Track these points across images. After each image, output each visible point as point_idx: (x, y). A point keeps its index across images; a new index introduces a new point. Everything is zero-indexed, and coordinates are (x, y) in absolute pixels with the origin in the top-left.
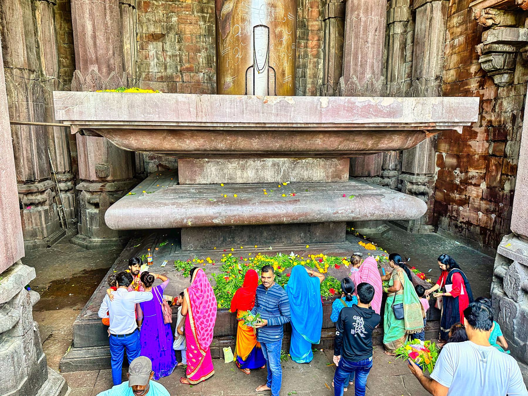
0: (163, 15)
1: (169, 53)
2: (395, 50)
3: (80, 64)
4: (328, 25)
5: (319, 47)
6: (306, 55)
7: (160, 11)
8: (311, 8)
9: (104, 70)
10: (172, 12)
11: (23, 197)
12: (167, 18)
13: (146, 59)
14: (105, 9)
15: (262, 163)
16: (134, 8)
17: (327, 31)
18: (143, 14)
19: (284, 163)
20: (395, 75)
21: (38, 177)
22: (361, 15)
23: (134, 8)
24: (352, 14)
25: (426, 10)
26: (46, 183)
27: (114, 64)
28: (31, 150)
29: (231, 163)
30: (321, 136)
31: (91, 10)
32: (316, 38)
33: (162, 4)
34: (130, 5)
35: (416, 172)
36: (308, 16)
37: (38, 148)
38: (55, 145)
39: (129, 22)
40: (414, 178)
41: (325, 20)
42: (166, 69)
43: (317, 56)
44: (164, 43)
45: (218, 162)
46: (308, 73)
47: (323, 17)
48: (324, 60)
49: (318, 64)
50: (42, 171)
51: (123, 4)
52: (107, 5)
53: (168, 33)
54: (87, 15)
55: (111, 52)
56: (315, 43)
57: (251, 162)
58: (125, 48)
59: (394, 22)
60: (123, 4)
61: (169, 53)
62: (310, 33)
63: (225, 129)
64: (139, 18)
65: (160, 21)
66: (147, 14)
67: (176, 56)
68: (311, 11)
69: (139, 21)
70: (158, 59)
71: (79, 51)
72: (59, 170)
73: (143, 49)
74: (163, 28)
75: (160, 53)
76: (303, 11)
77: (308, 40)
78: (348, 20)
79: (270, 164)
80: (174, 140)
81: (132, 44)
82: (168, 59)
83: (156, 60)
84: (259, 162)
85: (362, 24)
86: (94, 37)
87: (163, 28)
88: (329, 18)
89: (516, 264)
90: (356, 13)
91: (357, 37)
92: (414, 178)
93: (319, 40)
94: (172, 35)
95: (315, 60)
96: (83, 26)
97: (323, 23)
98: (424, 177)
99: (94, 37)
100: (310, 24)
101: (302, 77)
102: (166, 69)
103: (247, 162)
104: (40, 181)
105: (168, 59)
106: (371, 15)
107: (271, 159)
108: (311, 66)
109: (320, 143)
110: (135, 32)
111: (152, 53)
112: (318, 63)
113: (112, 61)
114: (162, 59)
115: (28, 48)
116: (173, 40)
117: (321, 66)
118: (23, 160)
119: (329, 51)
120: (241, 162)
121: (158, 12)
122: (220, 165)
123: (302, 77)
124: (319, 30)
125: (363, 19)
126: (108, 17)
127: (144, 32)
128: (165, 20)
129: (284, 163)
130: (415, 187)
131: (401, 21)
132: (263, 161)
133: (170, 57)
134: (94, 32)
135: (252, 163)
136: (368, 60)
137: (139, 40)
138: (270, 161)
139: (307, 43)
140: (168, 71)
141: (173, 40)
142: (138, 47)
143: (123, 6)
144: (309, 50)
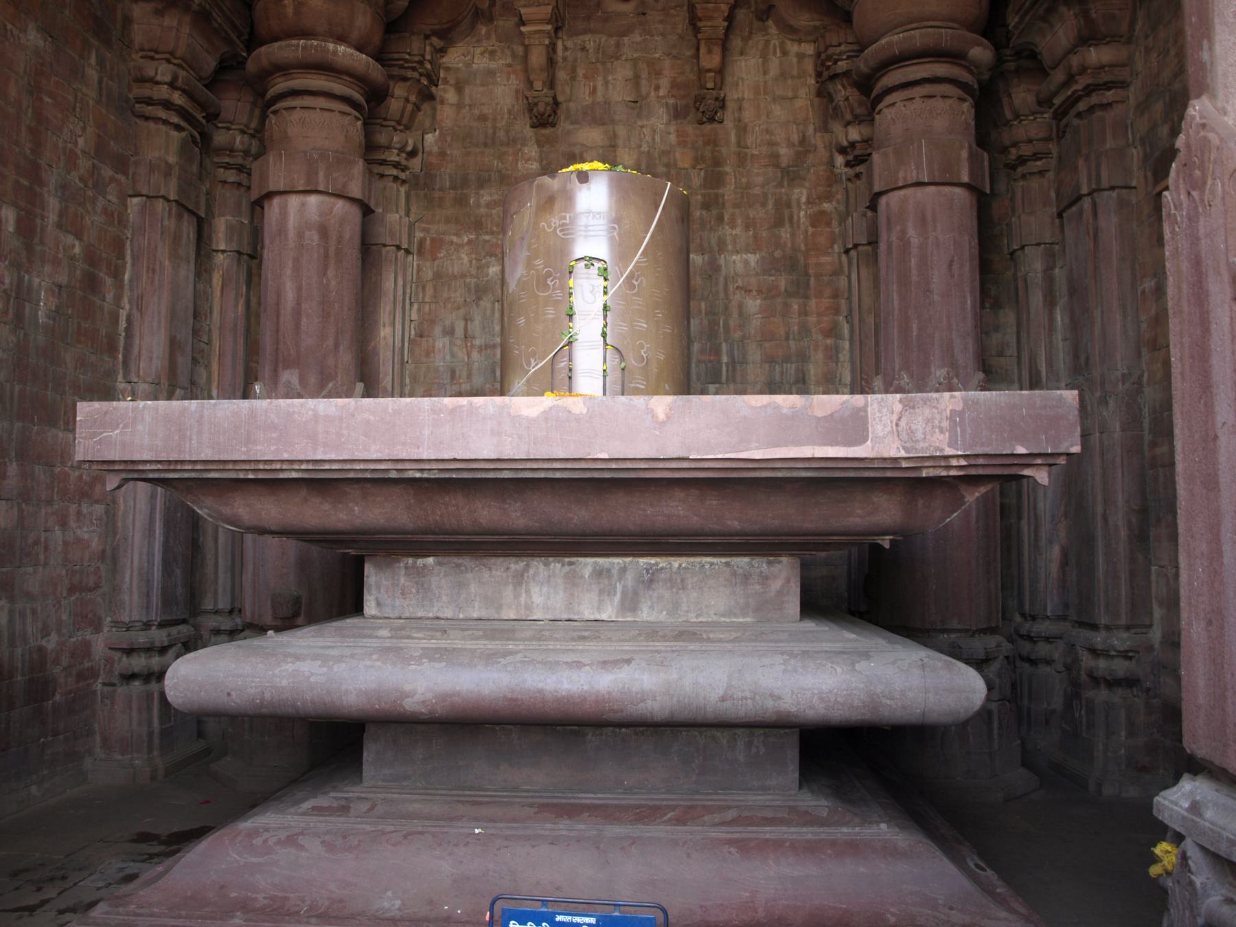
0: (471, 262)
1: (477, 342)
2: (1032, 311)
3: (266, 371)
4: (855, 261)
5: (837, 311)
6: (805, 330)
7: (463, 256)
8: (813, 225)
9: (313, 379)
10: (491, 256)
11: (120, 659)
12: (478, 268)
13: (428, 355)
14: (326, 256)
15: (567, 569)
16: (408, 252)
17: (854, 277)
18: (428, 264)
19: (624, 570)
20: (1038, 373)
21: (155, 616)
22: (911, 232)
23: (408, 252)
24: (889, 229)
25: (1081, 212)
26: (174, 630)
27: (336, 366)
28: (151, 554)
29: (490, 569)
30: (679, 494)
31: (297, 260)
32: (828, 292)
33: (470, 242)
34: (399, 248)
35: (1103, 620)
36: (806, 245)
37: (166, 549)
38: (216, 548)
39: (391, 283)
40: (1099, 639)
41: (847, 251)
42: (469, 376)
43: (832, 331)
44: (467, 319)
45: (458, 566)
46: (812, 372)
47: (844, 244)
48: (851, 340)
49: (837, 352)
50: (168, 600)
51: (385, 245)
52: (332, 250)
53: (479, 299)
54: (288, 272)
55: (330, 342)
56: (826, 302)
57: (538, 567)
58: (382, 334)
59: (1022, 248)
60: (385, 245)
61: (477, 342)
62: (812, 281)
63: (425, 475)
64: (418, 272)
65: (463, 276)
66: (436, 262)
67: (494, 346)
68: (814, 234)
69: (419, 277)
70: (453, 355)
71: (267, 341)
72: (221, 606)
73: (421, 336)
74: (469, 290)
75: (459, 342)
76: (793, 235)
77: (807, 297)
78: (883, 246)
79: (587, 572)
80: (327, 506)
81: (398, 326)
82: (475, 355)
83: (448, 357)
84: (559, 566)
85: (914, 251)
86: (297, 313)
87: (469, 290)
88: (856, 246)
89: (1188, 845)
90: (898, 228)
91: (904, 280)
92: (1099, 639)
93: (835, 296)
94: (486, 303)
95: (829, 341)
96: (279, 294)
97: (844, 258)
98: (1125, 635)
99: (297, 313)
100: (813, 261)
101: (797, 382)
102: (469, 376)
103: (528, 565)
104: (161, 625)
105: (475, 355)
106: (935, 230)
107: (590, 560)
108: (820, 356)
109: (676, 511)
110: (408, 301)
111: (441, 343)
112: (837, 349)
113: (330, 361)
114: (462, 355)
115: (174, 345)
116: (488, 313)
117: (845, 355)
118: (131, 576)
119: (860, 321)
120: (513, 567)
121: (459, 258)
122: (462, 572)
123: (797, 382)
124: (837, 272)
125: (915, 241)
126: (331, 273)
127: (427, 300)
128: (474, 272)
129: (624, 570)
130: (1102, 663)
131: (1038, 245)
132: (571, 564)
133: (480, 350)
134: (299, 304)
135: (541, 566)
136: (937, 335)
137: (414, 316)
138: (587, 565)
139: (805, 305)
140: (474, 380)
141: (488, 313)
142: (413, 332)
143: (384, 250)
144: (812, 319)
